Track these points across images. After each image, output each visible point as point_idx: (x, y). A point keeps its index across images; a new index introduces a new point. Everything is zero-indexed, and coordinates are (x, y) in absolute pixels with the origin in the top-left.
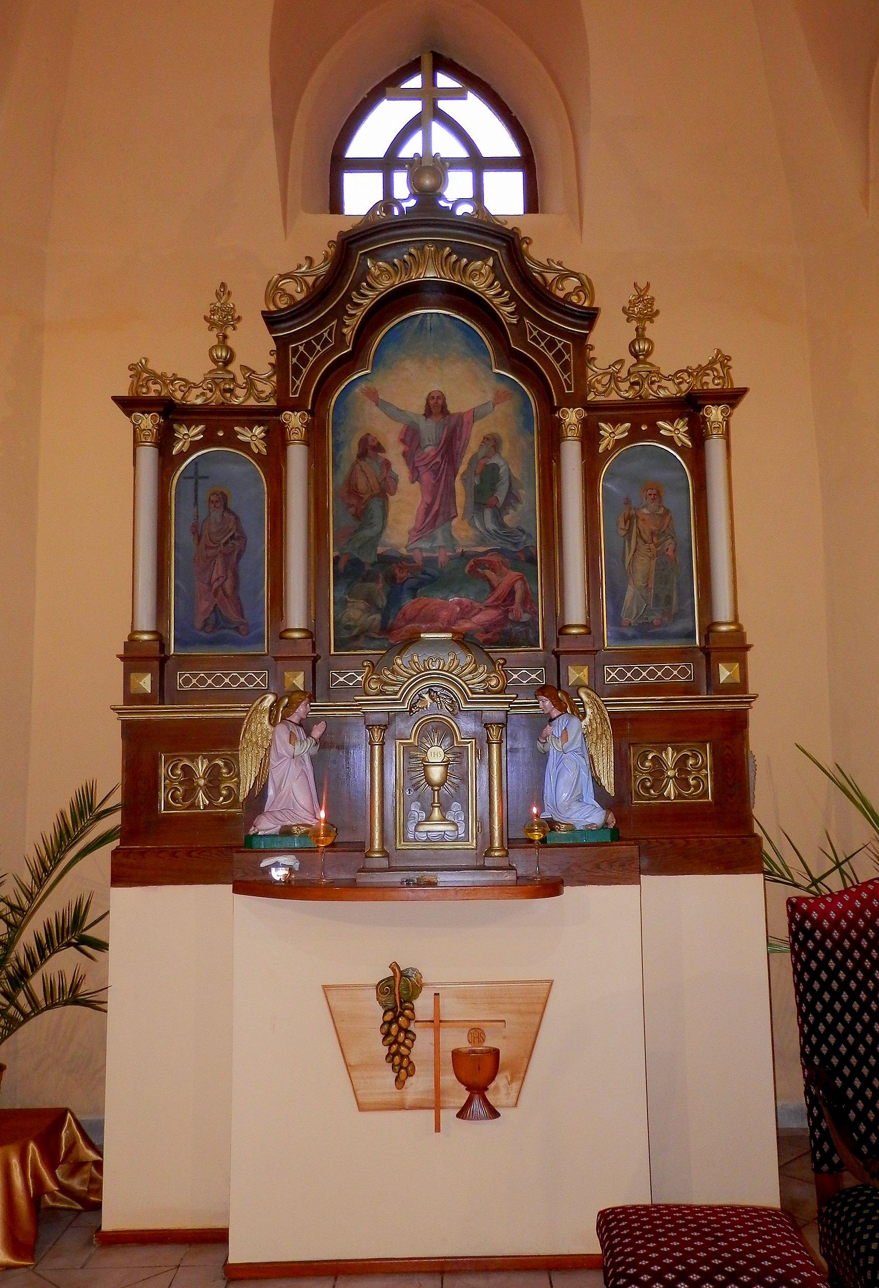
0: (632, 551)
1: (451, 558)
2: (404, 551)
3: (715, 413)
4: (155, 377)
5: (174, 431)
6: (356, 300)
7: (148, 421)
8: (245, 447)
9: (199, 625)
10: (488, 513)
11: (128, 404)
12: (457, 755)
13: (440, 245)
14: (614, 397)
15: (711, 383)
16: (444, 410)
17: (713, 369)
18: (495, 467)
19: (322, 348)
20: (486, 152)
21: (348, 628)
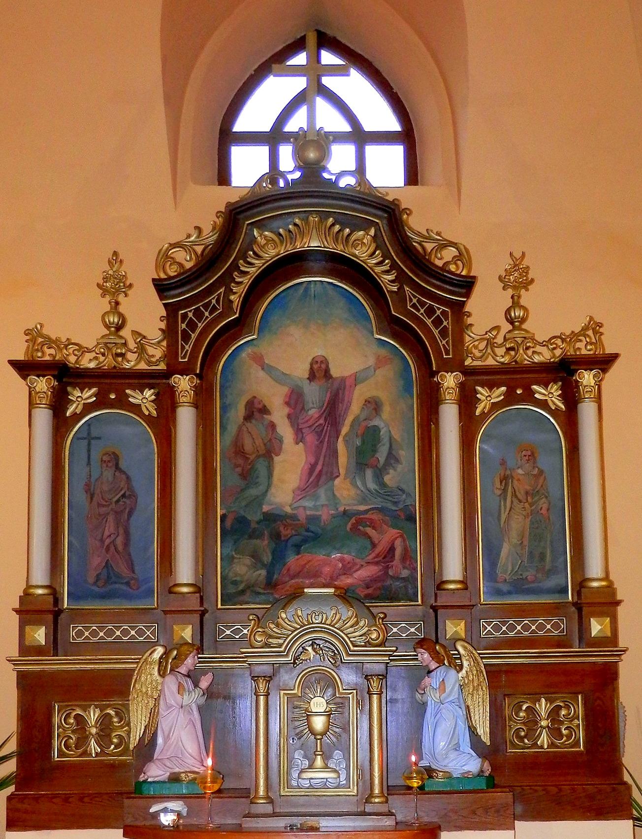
0: (508, 509)
1: (333, 516)
2: (288, 510)
3: (587, 378)
4: (50, 342)
5: (68, 394)
6: (242, 269)
7: (43, 384)
8: (136, 409)
9: (91, 580)
10: (369, 473)
11: (24, 368)
12: (338, 706)
13: (326, 215)
14: (490, 362)
15: (584, 349)
16: (327, 374)
17: (585, 336)
18: (376, 429)
19: (210, 314)
20: (369, 126)
21: (235, 583)
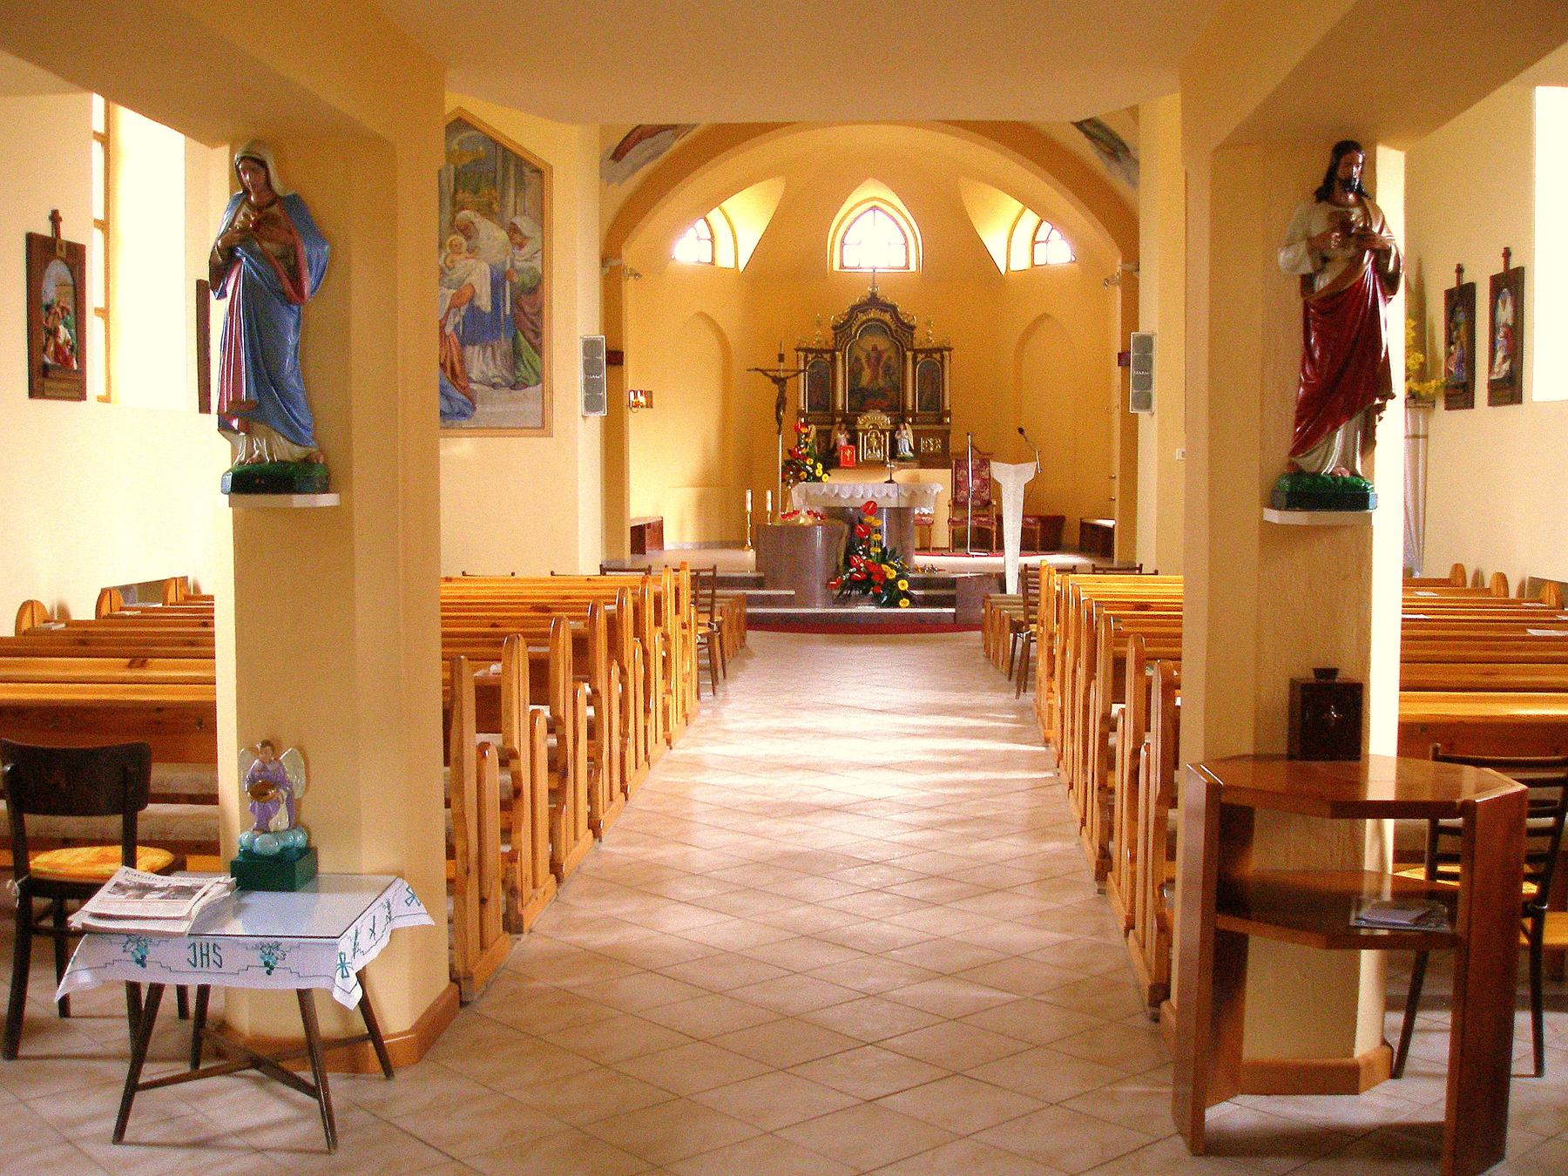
3: (946, 353)
7: (802, 354)
